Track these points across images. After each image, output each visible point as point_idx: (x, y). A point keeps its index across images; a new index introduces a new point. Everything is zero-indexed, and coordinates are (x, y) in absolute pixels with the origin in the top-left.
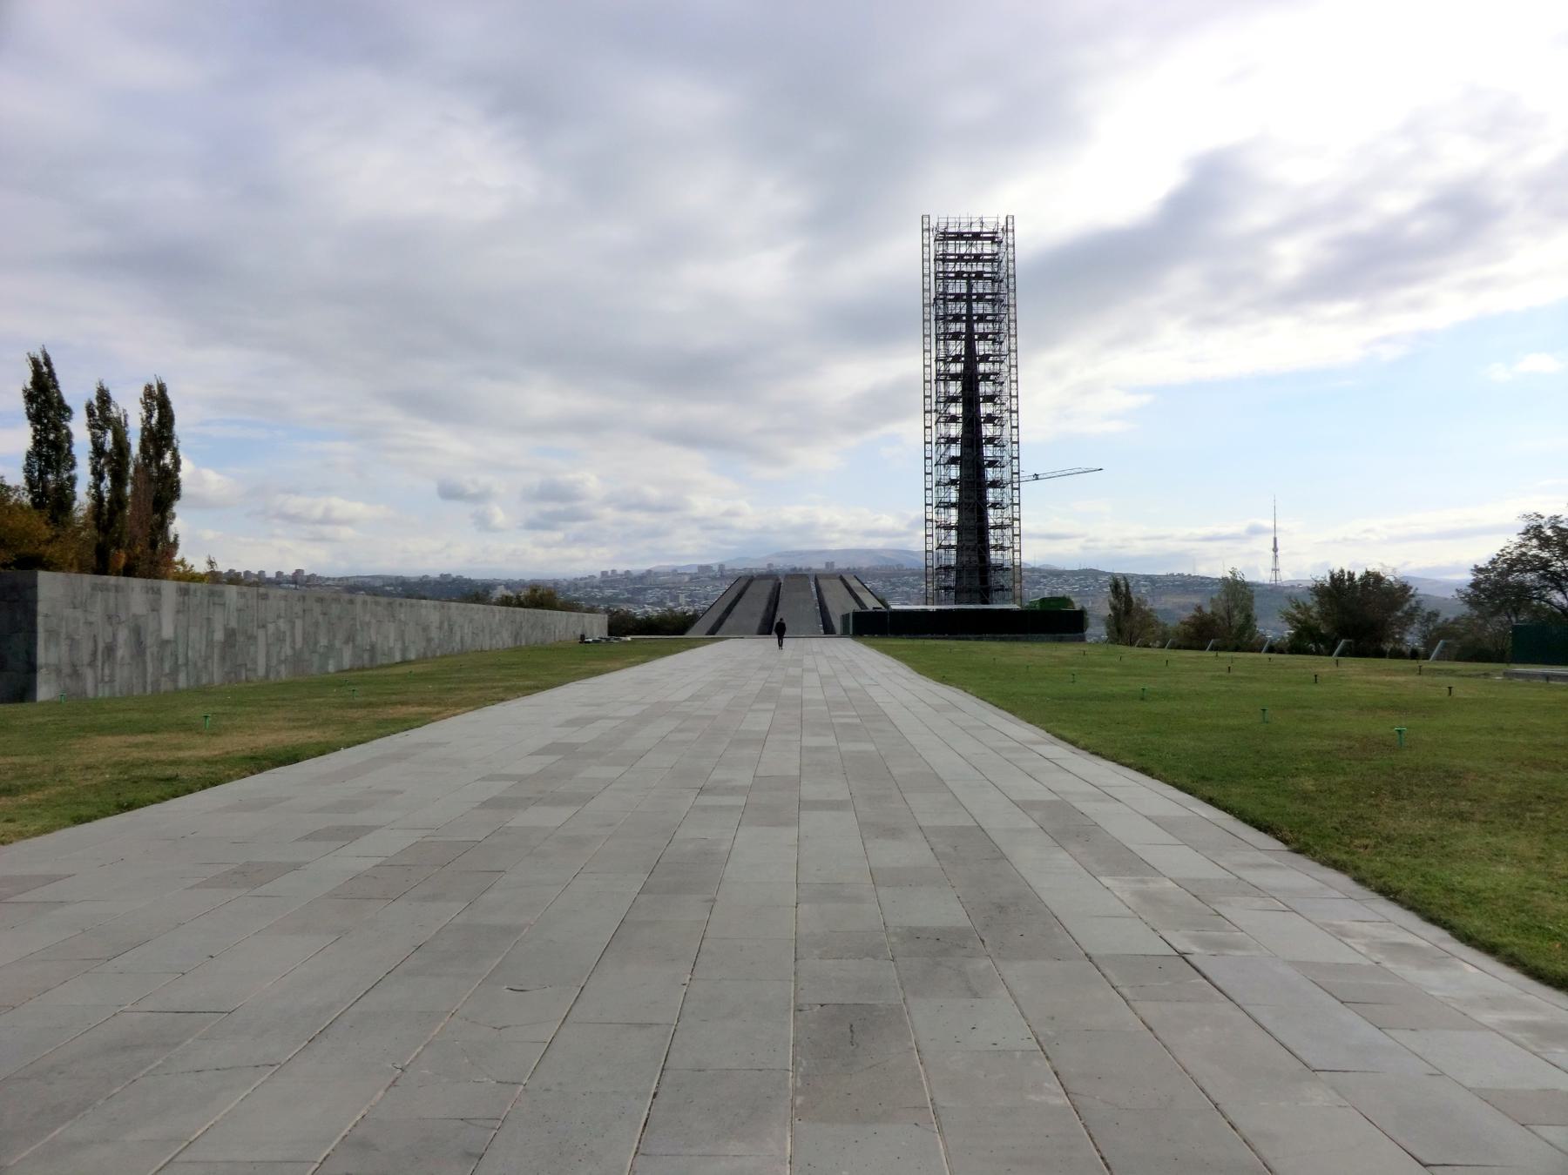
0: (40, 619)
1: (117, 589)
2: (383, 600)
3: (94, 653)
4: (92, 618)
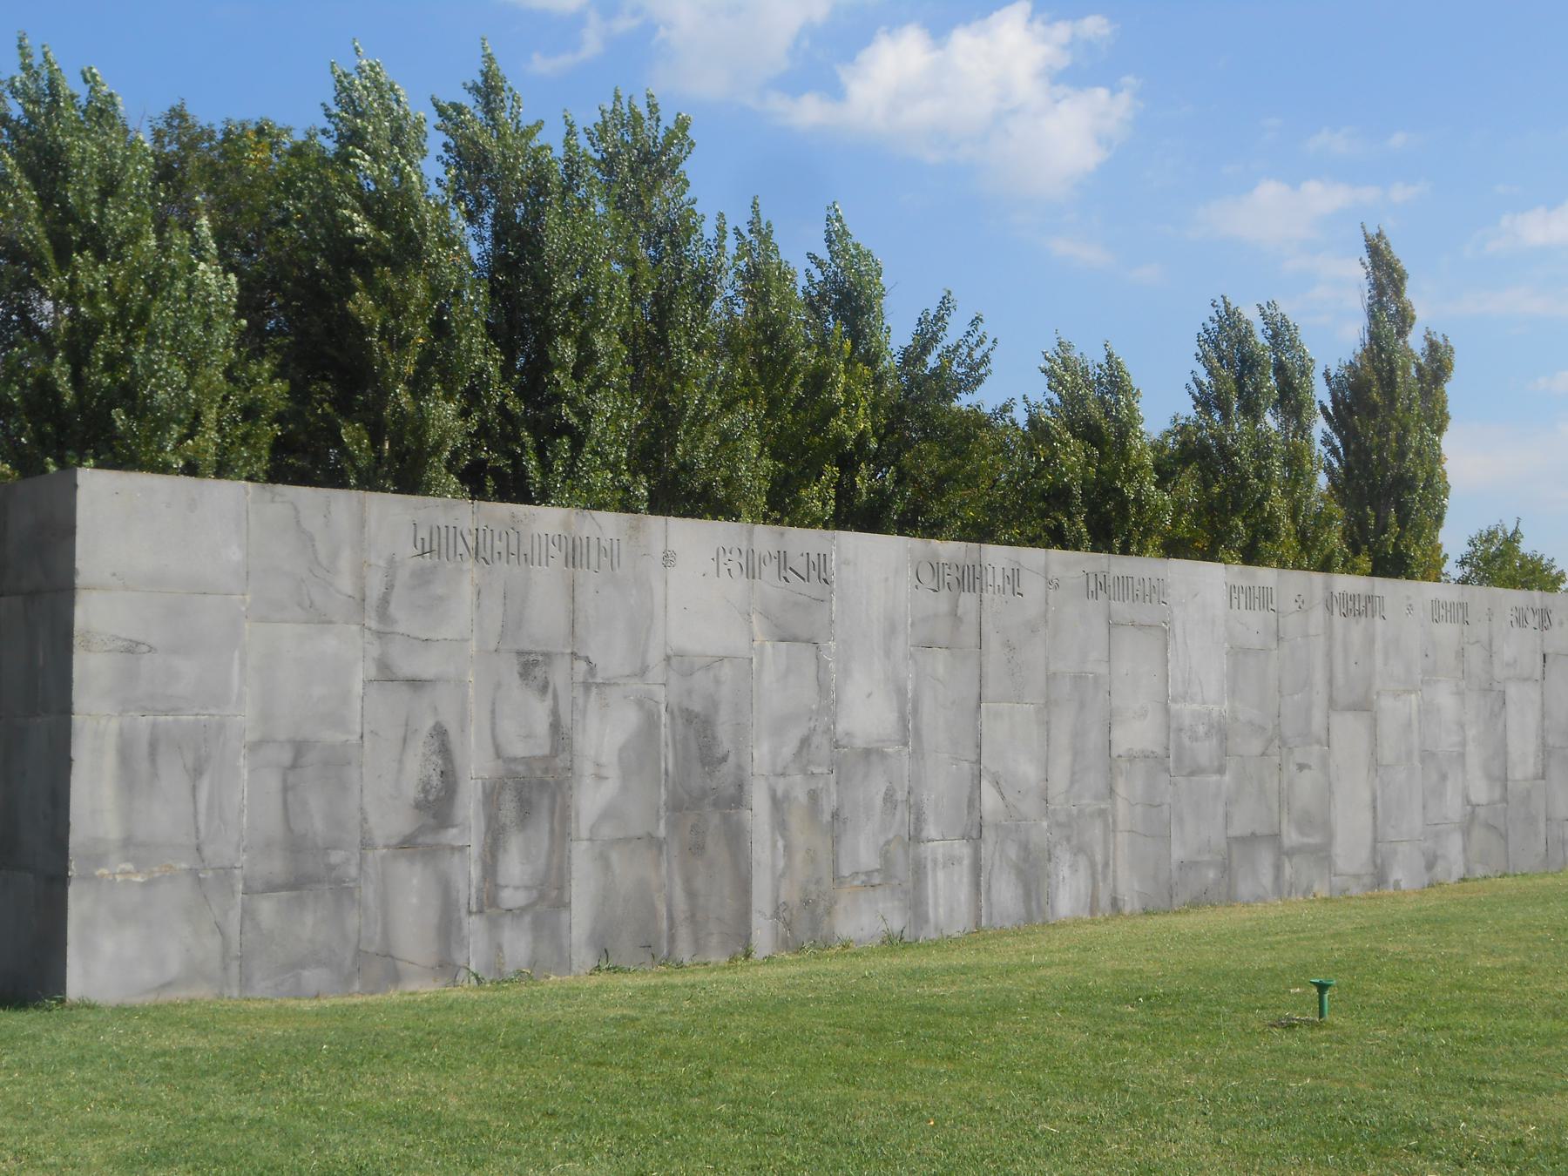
0: (91, 670)
3: (437, 806)
4: (409, 665)
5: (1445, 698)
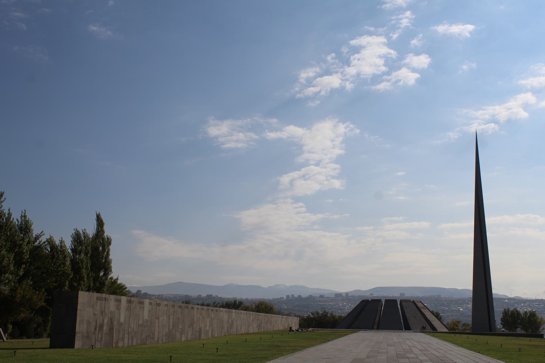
1: (105, 299)
2: (205, 308)
3: (95, 328)
5: (165, 318)
